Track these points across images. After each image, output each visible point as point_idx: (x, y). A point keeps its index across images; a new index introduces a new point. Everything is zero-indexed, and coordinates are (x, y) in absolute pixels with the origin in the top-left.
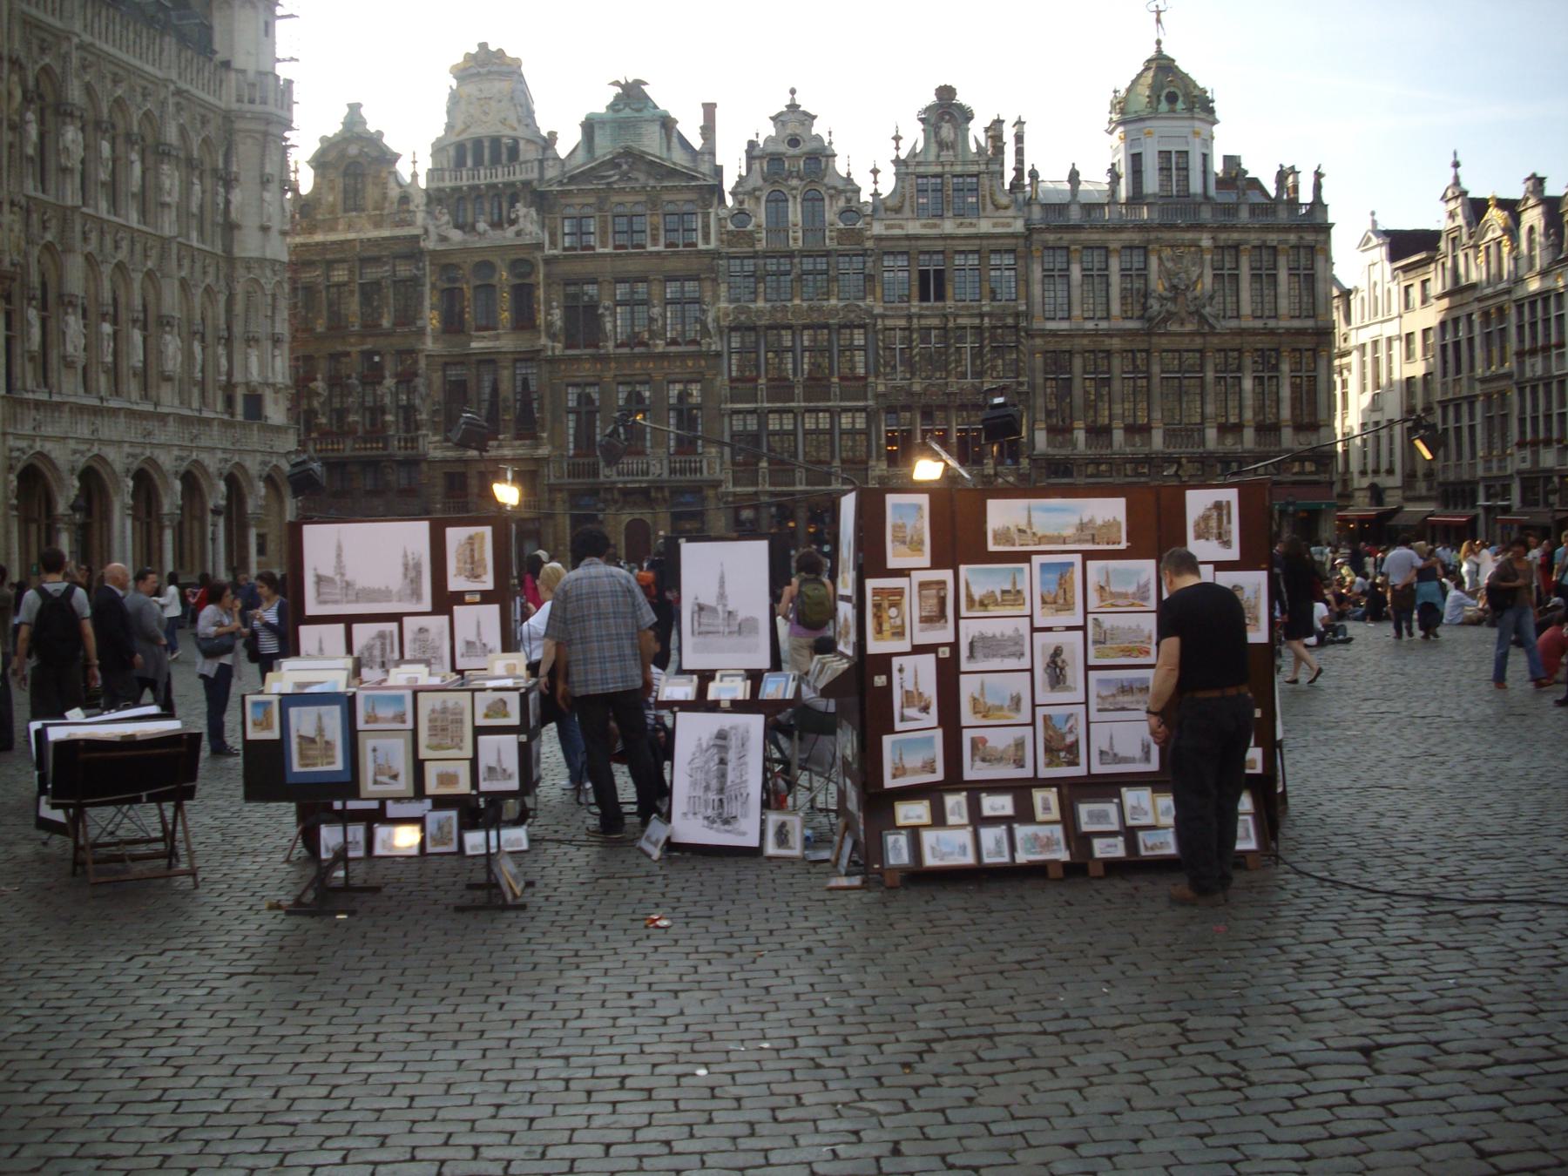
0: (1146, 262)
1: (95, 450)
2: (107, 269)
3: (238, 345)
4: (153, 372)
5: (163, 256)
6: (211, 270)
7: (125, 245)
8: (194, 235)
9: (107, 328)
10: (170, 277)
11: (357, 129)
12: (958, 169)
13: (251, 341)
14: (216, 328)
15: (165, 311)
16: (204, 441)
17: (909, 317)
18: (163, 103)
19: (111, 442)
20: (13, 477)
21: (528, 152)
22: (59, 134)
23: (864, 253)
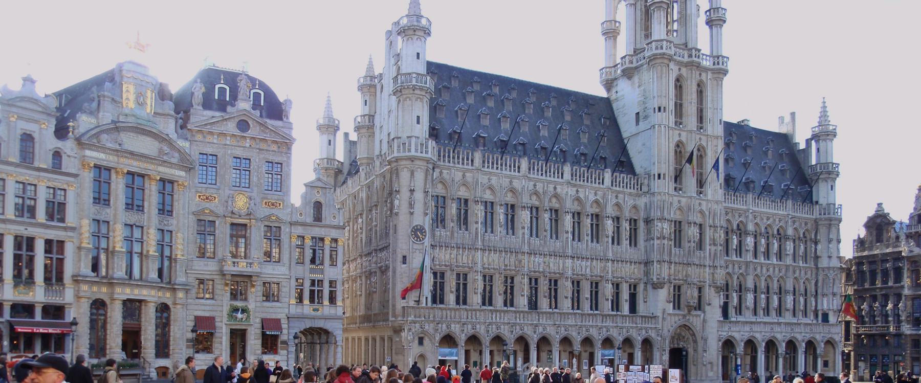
2: (763, 279)
3: (819, 296)
4: (783, 308)
5: (787, 270)
6: (809, 272)
7: (771, 269)
9: (763, 296)
20: (720, 344)
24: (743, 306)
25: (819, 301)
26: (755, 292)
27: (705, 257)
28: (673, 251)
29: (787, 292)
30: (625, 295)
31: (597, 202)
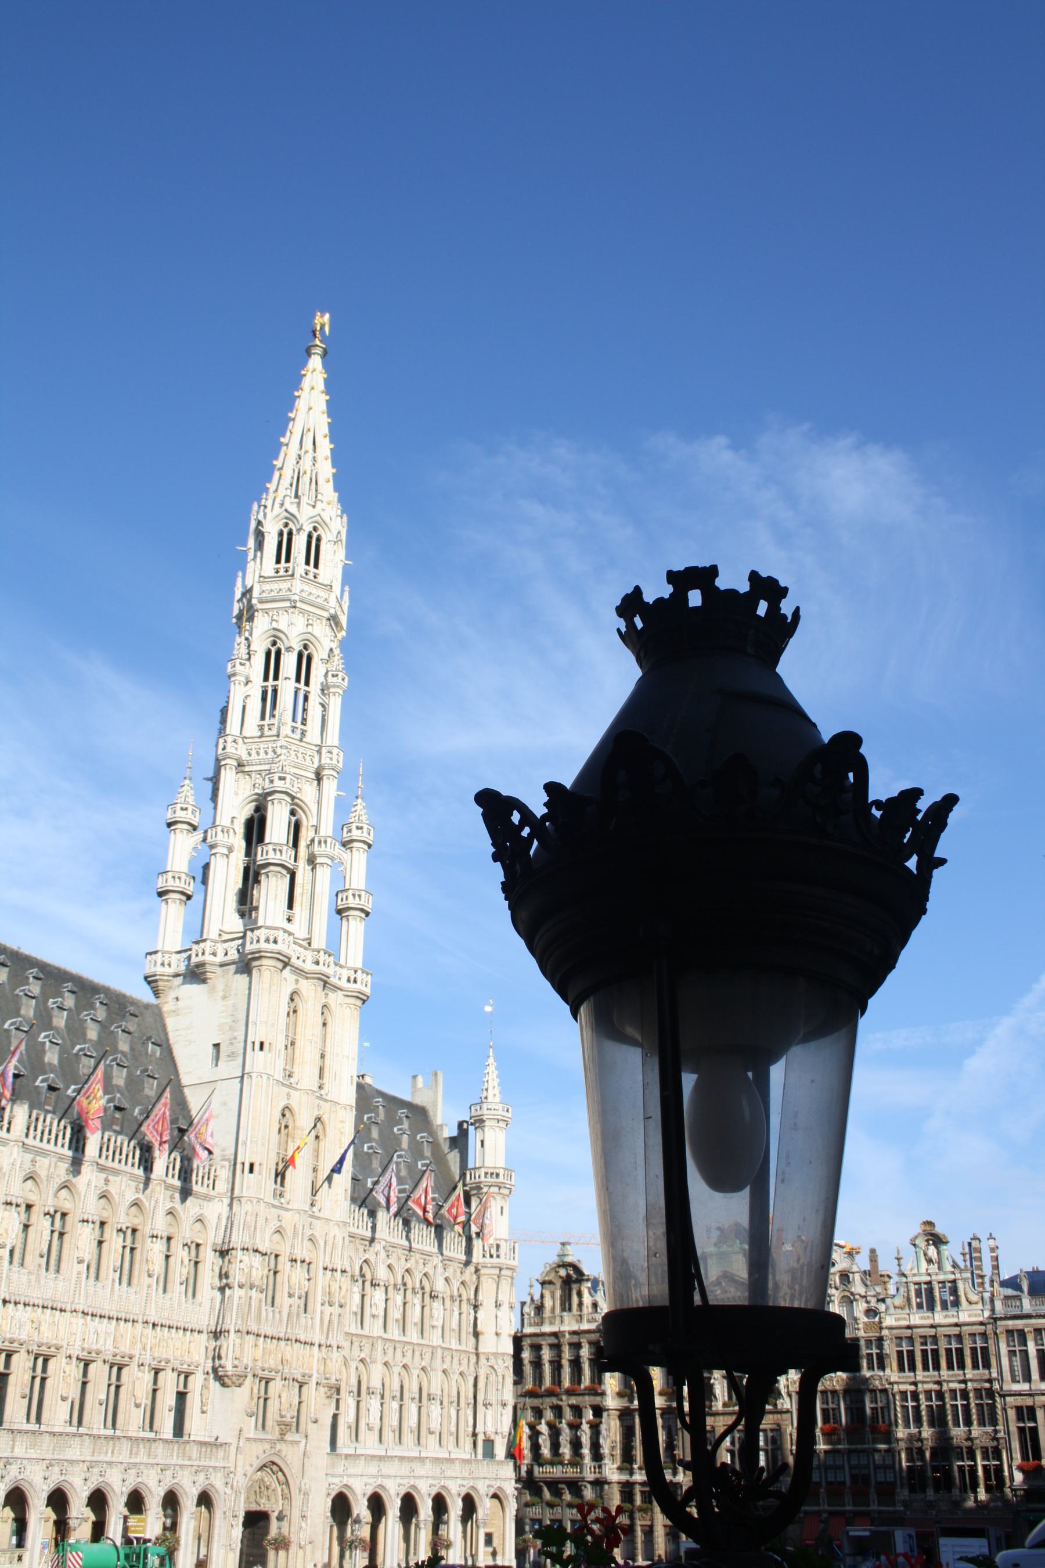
1: (379, 1482)
7: (409, 1354)
8: (453, 1341)
10: (435, 1370)
11: (569, 1259)
12: (941, 1277)
15: (432, 1391)
16: (449, 1473)
19: (389, 1476)
26: (382, 1397)
27: (312, 1327)
28: (264, 1313)
30: (167, 1400)
31: (136, 1204)
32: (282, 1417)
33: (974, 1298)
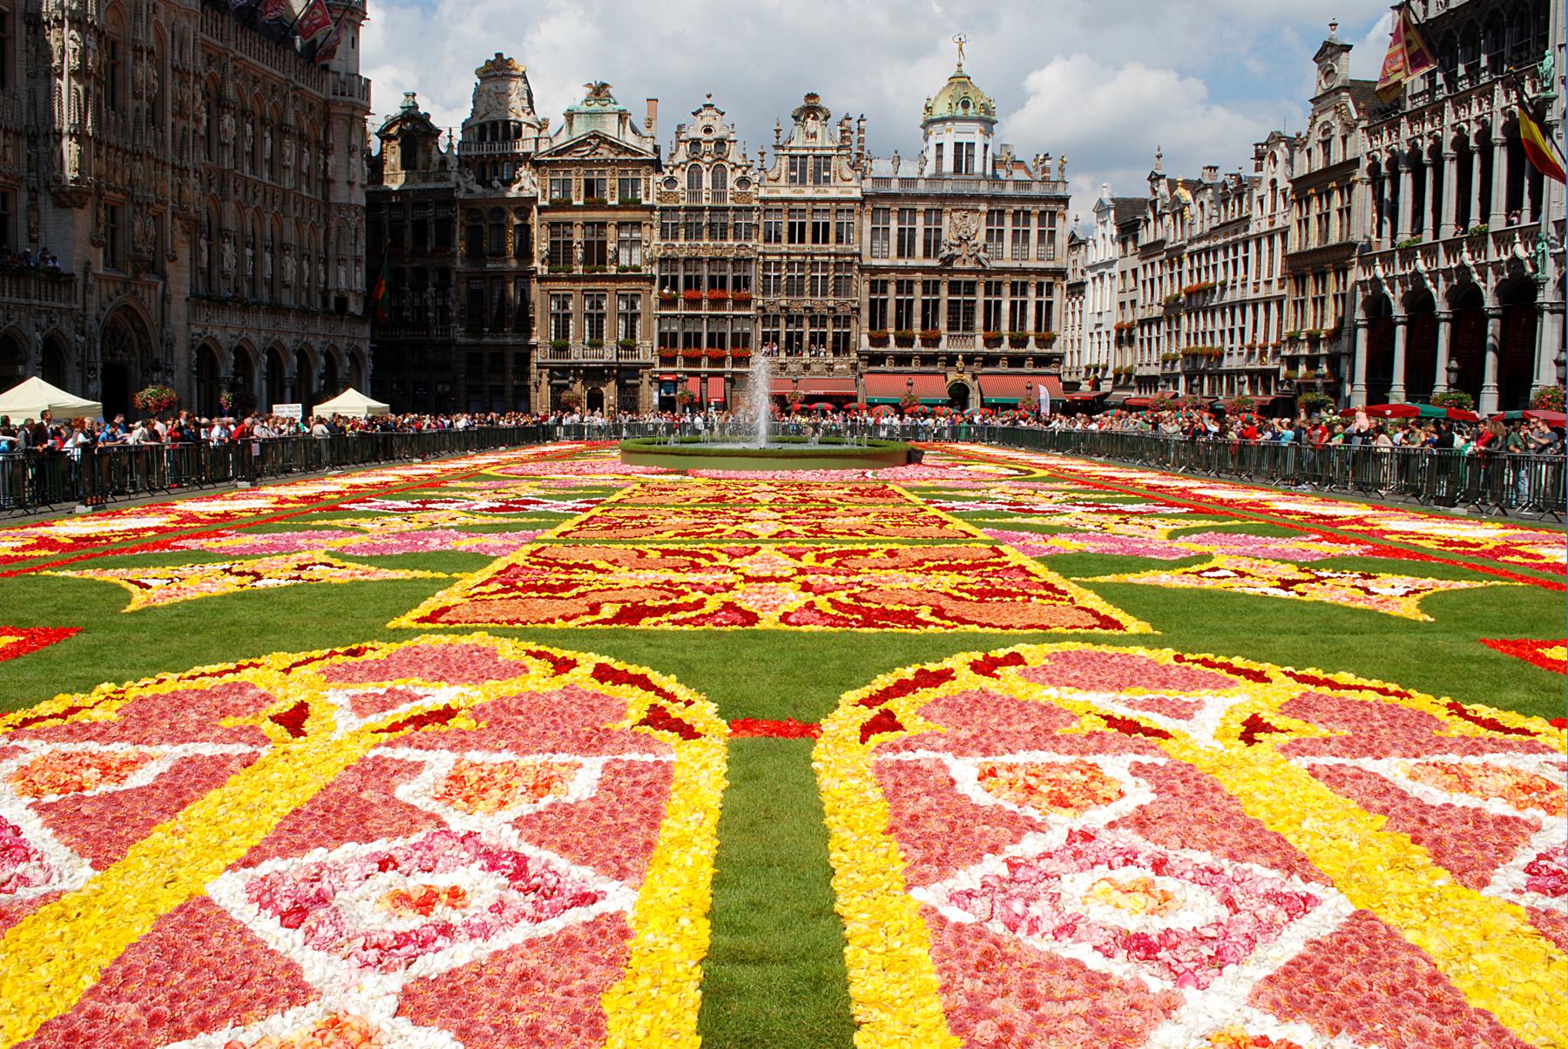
0: (939, 221)
7: (260, 195)
9: (249, 252)
12: (818, 152)
13: (340, 261)
14: (318, 251)
16: (311, 330)
17: (781, 255)
18: (285, 98)
21: (528, 133)
22: (219, 121)
23: (751, 209)
24: (215, 272)
25: (330, 272)
27: (164, 143)
29: (284, 247)
32: (135, 249)
33: (848, 174)
